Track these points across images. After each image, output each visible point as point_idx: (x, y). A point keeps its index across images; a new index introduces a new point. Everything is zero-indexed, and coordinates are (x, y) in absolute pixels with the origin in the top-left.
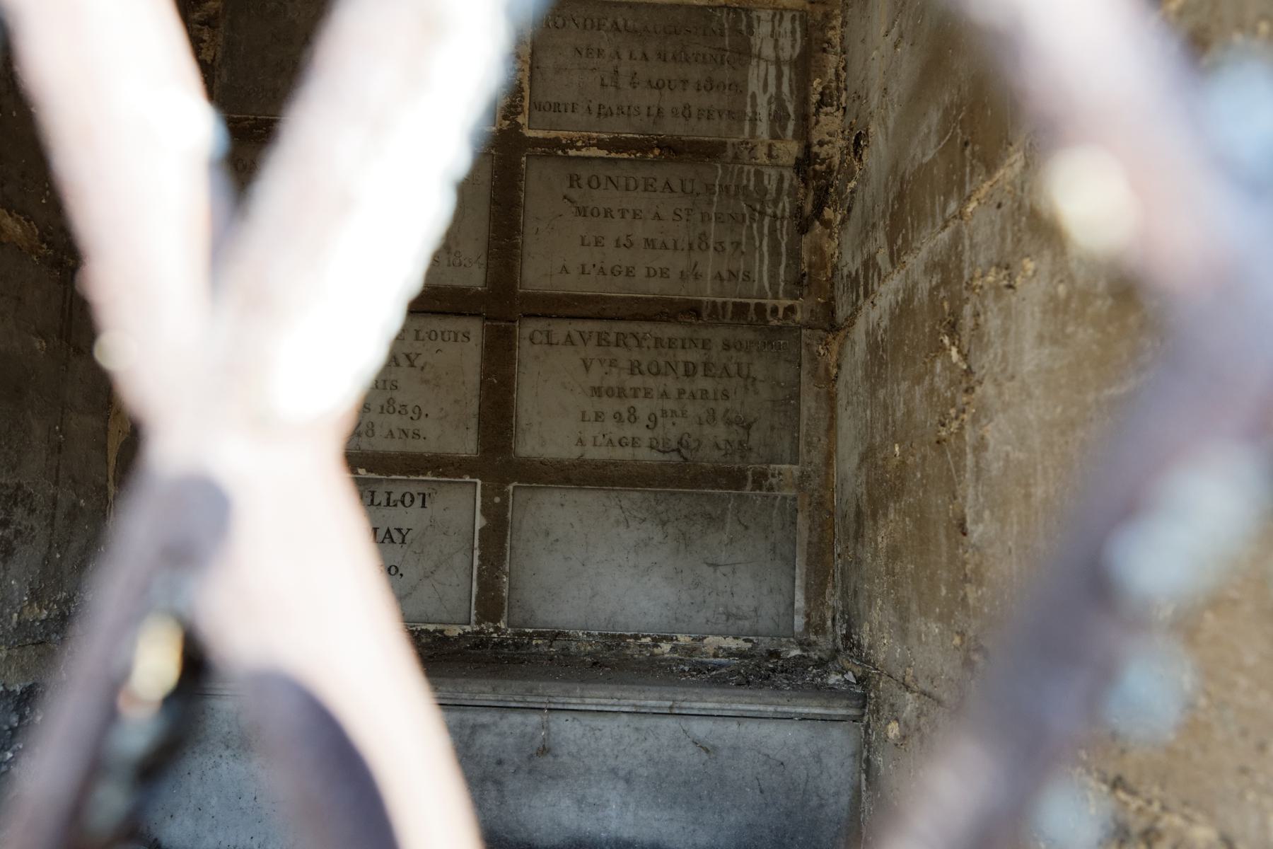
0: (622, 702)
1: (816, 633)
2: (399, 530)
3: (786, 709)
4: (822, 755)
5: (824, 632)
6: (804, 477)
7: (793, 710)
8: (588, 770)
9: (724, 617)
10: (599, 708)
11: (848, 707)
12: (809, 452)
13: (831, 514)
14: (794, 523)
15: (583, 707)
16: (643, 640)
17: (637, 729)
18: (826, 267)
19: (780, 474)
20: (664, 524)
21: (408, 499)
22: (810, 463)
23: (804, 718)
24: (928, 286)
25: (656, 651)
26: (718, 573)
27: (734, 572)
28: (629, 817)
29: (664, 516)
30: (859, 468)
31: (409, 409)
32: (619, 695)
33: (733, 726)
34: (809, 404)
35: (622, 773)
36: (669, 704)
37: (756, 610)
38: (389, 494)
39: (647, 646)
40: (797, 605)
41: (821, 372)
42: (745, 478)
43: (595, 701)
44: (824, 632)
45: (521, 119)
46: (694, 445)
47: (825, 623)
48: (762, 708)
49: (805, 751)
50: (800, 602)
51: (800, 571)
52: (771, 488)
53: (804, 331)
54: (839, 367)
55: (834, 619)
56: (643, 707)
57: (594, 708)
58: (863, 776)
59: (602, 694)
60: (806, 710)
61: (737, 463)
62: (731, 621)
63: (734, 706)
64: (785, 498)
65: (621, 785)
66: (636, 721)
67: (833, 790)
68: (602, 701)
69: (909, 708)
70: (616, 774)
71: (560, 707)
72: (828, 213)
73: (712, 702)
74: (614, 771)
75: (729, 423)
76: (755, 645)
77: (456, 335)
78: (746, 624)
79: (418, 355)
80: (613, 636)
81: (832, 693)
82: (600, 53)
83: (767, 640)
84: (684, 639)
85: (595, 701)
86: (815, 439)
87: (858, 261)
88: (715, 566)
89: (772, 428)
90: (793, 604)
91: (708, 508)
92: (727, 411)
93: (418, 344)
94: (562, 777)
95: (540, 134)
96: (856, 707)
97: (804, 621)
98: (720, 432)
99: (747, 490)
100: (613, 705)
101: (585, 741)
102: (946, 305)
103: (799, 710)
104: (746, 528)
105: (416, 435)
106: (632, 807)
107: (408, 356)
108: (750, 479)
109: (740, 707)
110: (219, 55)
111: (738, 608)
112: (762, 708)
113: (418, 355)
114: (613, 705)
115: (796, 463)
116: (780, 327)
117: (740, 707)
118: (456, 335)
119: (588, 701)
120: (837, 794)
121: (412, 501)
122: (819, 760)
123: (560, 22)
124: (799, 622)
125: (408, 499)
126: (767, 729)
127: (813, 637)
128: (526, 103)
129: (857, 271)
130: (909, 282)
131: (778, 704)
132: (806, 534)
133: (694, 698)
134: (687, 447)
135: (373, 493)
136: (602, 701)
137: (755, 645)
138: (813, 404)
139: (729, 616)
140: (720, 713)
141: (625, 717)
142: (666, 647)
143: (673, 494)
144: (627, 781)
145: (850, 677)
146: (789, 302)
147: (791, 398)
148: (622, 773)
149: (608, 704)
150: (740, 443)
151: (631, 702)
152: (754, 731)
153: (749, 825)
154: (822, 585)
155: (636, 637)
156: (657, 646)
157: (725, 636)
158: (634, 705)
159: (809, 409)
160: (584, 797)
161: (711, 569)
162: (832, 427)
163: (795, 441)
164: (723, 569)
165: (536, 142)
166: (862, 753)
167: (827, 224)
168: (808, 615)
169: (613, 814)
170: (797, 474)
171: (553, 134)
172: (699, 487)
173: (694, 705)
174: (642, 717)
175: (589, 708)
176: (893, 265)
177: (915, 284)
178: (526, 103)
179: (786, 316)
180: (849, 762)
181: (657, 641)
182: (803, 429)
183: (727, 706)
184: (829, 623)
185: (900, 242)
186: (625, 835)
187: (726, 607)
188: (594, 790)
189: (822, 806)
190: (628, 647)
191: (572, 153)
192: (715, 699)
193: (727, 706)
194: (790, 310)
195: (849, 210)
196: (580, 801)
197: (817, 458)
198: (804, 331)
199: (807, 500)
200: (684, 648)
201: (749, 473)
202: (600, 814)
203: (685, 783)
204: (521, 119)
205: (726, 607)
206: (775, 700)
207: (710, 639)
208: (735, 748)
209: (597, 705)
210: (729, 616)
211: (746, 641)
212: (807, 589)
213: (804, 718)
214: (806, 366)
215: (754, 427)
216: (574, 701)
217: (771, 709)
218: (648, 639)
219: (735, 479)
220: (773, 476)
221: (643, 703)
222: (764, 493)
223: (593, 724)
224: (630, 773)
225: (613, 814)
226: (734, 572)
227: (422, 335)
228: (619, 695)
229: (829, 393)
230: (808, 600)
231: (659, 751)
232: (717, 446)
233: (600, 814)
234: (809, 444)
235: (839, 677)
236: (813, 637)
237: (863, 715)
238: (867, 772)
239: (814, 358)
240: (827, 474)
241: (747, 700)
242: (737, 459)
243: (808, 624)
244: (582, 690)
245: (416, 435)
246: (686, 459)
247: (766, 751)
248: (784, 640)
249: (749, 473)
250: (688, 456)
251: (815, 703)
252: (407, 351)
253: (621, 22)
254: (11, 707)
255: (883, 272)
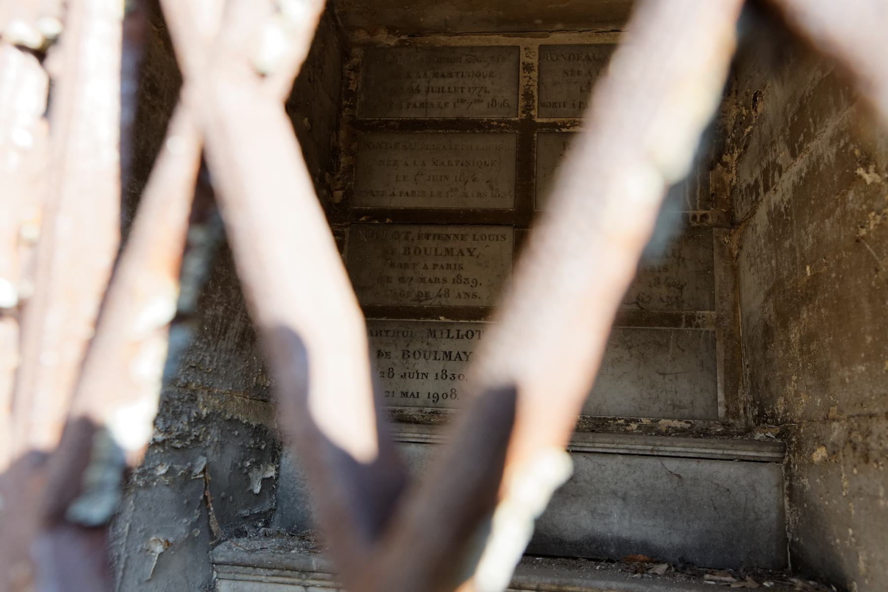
0: (620, 446)
1: (733, 418)
2: (465, 353)
3: (730, 452)
4: (756, 485)
5: (739, 417)
6: (719, 319)
7: (735, 453)
8: (598, 492)
9: (672, 407)
10: (604, 450)
11: (773, 451)
12: (722, 303)
13: (739, 342)
14: (715, 348)
15: (593, 450)
16: (619, 422)
17: (629, 465)
18: (725, 190)
19: (703, 317)
20: (630, 348)
21: (470, 334)
22: (723, 310)
23: (742, 460)
24: (834, 151)
25: (628, 428)
26: (667, 380)
27: (676, 378)
28: (626, 524)
29: (629, 344)
30: (766, 301)
31: (470, 280)
32: (617, 441)
33: (693, 464)
34: (720, 273)
35: (620, 494)
36: (650, 447)
37: (692, 403)
38: (458, 331)
39: (622, 425)
40: (719, 400)
41: (727, 253)
42: (681, 320)
43: (601, 445)
44: (739, 417)
45: (533, 113)
46: (647, 299)
47: (739, 412)
48: (713, 451)
49: (744, 483)
50: (721, 398)
51: (720, 377)
52: (698, 326)
53: (714, 229)
54: (740, 248)
55: (745, 409)
56: (632, 449)
57: (600, 450)
58: (786, 499)
59: (607, 440)
60: (744, 453)
61: (675, 310)
62: (676, 410)
63: (694, 450)
64: (707, 332)
65: (620, 502)
66: (627, 460)
67: (765, 509)
68: (607, 445)
69: (836, 433)
70: (616, 494)
71: (578, 449)
72: (726, 158)
73: (680, 447)
74: (614, 493)
75: (669, 286)
76: (693, 426)
77: (497, 237)
78: (686, 412)
79: (475, 249)
80: (600, 419)
81: (761, 443)
82: (579, 73)
83: (701, 422)
84: (645, 421)
85: (601, 445)
86: (725, 295)
87: (757, 173)
88: (664, 374)
89: (697, 288)
90: (717, 399)
91: (658, 339)
92: (667, 278)
93: (475, 242)
94: (581, 496)
95: (545, 120)
96: (779, 452)
97: (725, 410)
98: (663, 291)
99: (683, 327)
100: (614, 448)
101: (595, 472)
102: (857, 152)
103: (739, 453)
104: (683, 350)
105: (475, 296)
106: (627, 517)
107: (469, 250)
108: (684, 320)
109: (698, 450)
110: (360, 86)
111: (680, 401)
112: (713, 451)
113: (475, 249)
114: (614, 448)
115: (714, 310)
116: (699, 227)
117: (698, 450)
118: (497, 237)
119: (597, 445)
120: (768, 511)
121: (473, 335)
122: (754, 489)
123: (555, 58)
124: (721, 411)
125: (470, 334)
126: (717, 466)
127: (731, 421)
128: (536, 104)
129: (756, 181)
130: (814, 159)
131: (725, 449)
132: (722, 354)
133: (668, 444)
134: (643, 301)
135: (449, 331)
136: (607, 445)
137: (693, 426)
138: (723, 274)
139: (674, 406)
140: (684, 455)
141: (620, 457)
142: (634, 426)
143: (634, 330)
144: (624, 499)
145: (769, 434)
146: (704, 212)
147: (708, 270)
148: (620, 494)
149: (609, 447)
150: (677, 298)
151: (626, 446)
152: (707, 468)
153: (707, 531)
154: (736, 387)
155: (615, 420)
156: (628, 425)
157: (673, 419)
158: (627, 449)
159: (720, 277)
160: (595, 509)
161: (662, 376)
162: (736, 286)
163: (712, 296)
164: (668, 377)
165: (542, 125)
166: (783, 483)
167: (725, 165)
168: (727, 407)
169: (615, 521)
170: (714, 317)
171: (552, 120)
172: (651, 325)
173: (667, 448)
174: (632, 457)
175: (597, 450)
176: (794, 155)
177: (820, 157)
178: (536, 104)
179: (702, 221)
180: (775, 490)
181: (628, 422)
182: (717, 289)
183: (689, 450)
184: (742, 411)
185: (802, 137)
186: (624, 535)
187: (672, 400)
188: (602, 505)
189: (757, 519)
190: (609, 426)
191: (564, 130)
192: (682, 444)
193: (689, 450)
194: (704, 216)
195: (746, 147)
196: (593, 512)
197: (727, 306)
198: (714, 229)
199: (722, 334)
200: (646, 426)
201: (683, 316)
202: (607, 521)
203: (663, 502)
204: (533, 113)
205: (672, 400)
206: (723, 446)
207: (663, 421)
208: (695, 479)
209: (602, 448)
210: (674, 406)
211: (687, 422)
212: (725, 389)
213: (742, 460)
214: (717, 250)
215: (685, 288)
216: (588, 445)
217: (720, 452)
218: (622, 421)
219: (675, 321)
220: (699, 318)
221: (633, 447)
222: (693, 329)
223: (600, 462)
224: (625, 494)
225: (615, 521)
226: (676, 378)
227: (477, 237)
228: (617, 441)
229: (732, 266)
230: (726, 396)
231: (644, 480)
232: (661, 300)
233: (607, 521)
234: (721, 298)
235: (762, 435)
236: (731, 421)
237: (784, 458)
238: (790, 496)
239: (722, 245)
240: (734, 317)
241: (703, 445)
242: (675, 308)
243: (727, 412)
244: (594, 437)
245: (475, 296)
246: (642, 308)
247: (716, 482)
248: (712, 422)
249: (683, 316)
250: (644, 306)
251: (751, 448)
252: (469, 247)
253: (591, 55)
254: (250, 435)
255: (784, 167)
